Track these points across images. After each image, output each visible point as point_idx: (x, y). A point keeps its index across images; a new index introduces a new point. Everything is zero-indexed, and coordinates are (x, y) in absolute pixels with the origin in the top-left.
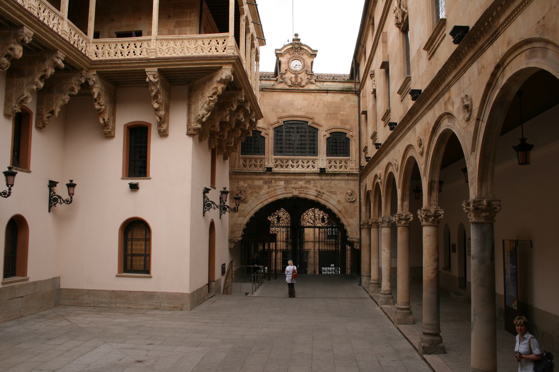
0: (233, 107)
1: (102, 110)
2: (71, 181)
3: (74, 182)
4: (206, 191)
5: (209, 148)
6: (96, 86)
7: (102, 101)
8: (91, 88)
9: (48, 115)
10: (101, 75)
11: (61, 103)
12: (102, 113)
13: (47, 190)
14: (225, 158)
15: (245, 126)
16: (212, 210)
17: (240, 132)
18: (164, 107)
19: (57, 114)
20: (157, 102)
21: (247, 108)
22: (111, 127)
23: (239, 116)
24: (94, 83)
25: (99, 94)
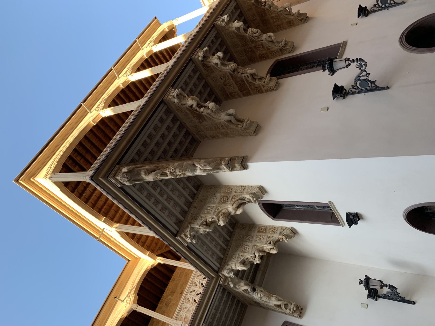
0: (193, 105)
1: (261, 254)
2: (361, 282)
3: (363, 279)
4: (339, 92)
5: (277, 86)
6: (234, 268)
7: (248, 256)
8: (237, 273)
9: (283, 307)
10: (223, 261)
11: (264, 299)
12: (265, 252)
13: (381, 300)
14: (303, 18)
15: (238, 29)
16: (370, 78)
17: (251, 30)
18: (223, 205)
19: (279, 303)
20: (218, 219)
21: (200, 59)
22: (280, 237)
23: (217, 64)
24: (233, 270)
25: (243, 263)
